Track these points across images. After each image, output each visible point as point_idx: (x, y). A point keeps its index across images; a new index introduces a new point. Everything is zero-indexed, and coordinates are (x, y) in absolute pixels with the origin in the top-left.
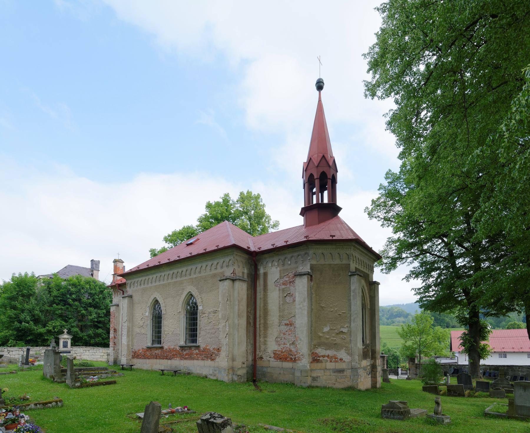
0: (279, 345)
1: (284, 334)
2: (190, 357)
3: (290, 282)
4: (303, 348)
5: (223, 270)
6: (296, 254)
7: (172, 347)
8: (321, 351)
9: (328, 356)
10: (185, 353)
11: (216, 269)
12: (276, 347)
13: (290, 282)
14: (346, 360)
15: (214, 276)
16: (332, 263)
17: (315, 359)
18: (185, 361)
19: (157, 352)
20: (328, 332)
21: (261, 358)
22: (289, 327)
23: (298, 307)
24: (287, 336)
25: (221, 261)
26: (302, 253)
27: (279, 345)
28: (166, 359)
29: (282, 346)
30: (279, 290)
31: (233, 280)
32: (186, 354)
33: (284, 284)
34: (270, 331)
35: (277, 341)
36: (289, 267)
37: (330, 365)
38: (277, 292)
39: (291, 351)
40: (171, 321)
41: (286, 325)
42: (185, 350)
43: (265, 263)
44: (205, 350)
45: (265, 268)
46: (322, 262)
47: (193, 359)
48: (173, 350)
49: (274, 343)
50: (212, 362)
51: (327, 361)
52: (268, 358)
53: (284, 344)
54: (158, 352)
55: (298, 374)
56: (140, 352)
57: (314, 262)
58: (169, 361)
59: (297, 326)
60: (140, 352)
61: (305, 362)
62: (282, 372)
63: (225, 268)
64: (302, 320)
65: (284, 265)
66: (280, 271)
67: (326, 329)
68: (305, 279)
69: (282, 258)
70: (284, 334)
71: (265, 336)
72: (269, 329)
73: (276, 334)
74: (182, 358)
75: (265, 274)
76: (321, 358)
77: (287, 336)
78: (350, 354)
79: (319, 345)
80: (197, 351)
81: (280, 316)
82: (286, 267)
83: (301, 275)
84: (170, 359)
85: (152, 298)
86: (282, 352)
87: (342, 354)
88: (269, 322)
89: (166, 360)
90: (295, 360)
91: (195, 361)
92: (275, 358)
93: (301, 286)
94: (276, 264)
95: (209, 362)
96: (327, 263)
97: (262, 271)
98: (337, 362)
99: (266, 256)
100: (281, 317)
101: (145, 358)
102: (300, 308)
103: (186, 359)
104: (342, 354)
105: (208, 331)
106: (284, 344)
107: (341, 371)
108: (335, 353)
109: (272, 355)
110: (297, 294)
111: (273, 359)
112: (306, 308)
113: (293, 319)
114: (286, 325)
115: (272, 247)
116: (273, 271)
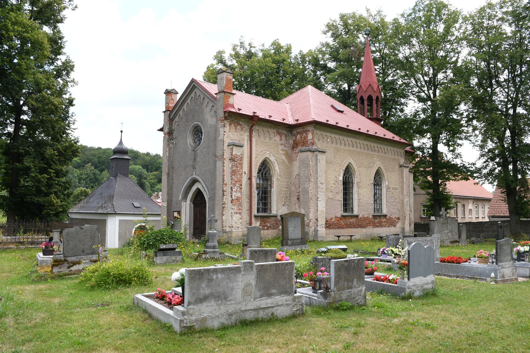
2: (381, 225)
7: (366, 216)
10: (376, 221)
19: (351, 220)
28: (361, 227)
32: (378, 222)
40: (365, 190)
47: (381, 226)
48: (367, 218)
54: (353, 220)
56: (333, 220)
58: (364, 230)
60: (333, 220)
74: (375, 226)
84: (364, 227)
89: (361, 229)
91: (384, 228)
101: (339, 228)
103: (377, 227)
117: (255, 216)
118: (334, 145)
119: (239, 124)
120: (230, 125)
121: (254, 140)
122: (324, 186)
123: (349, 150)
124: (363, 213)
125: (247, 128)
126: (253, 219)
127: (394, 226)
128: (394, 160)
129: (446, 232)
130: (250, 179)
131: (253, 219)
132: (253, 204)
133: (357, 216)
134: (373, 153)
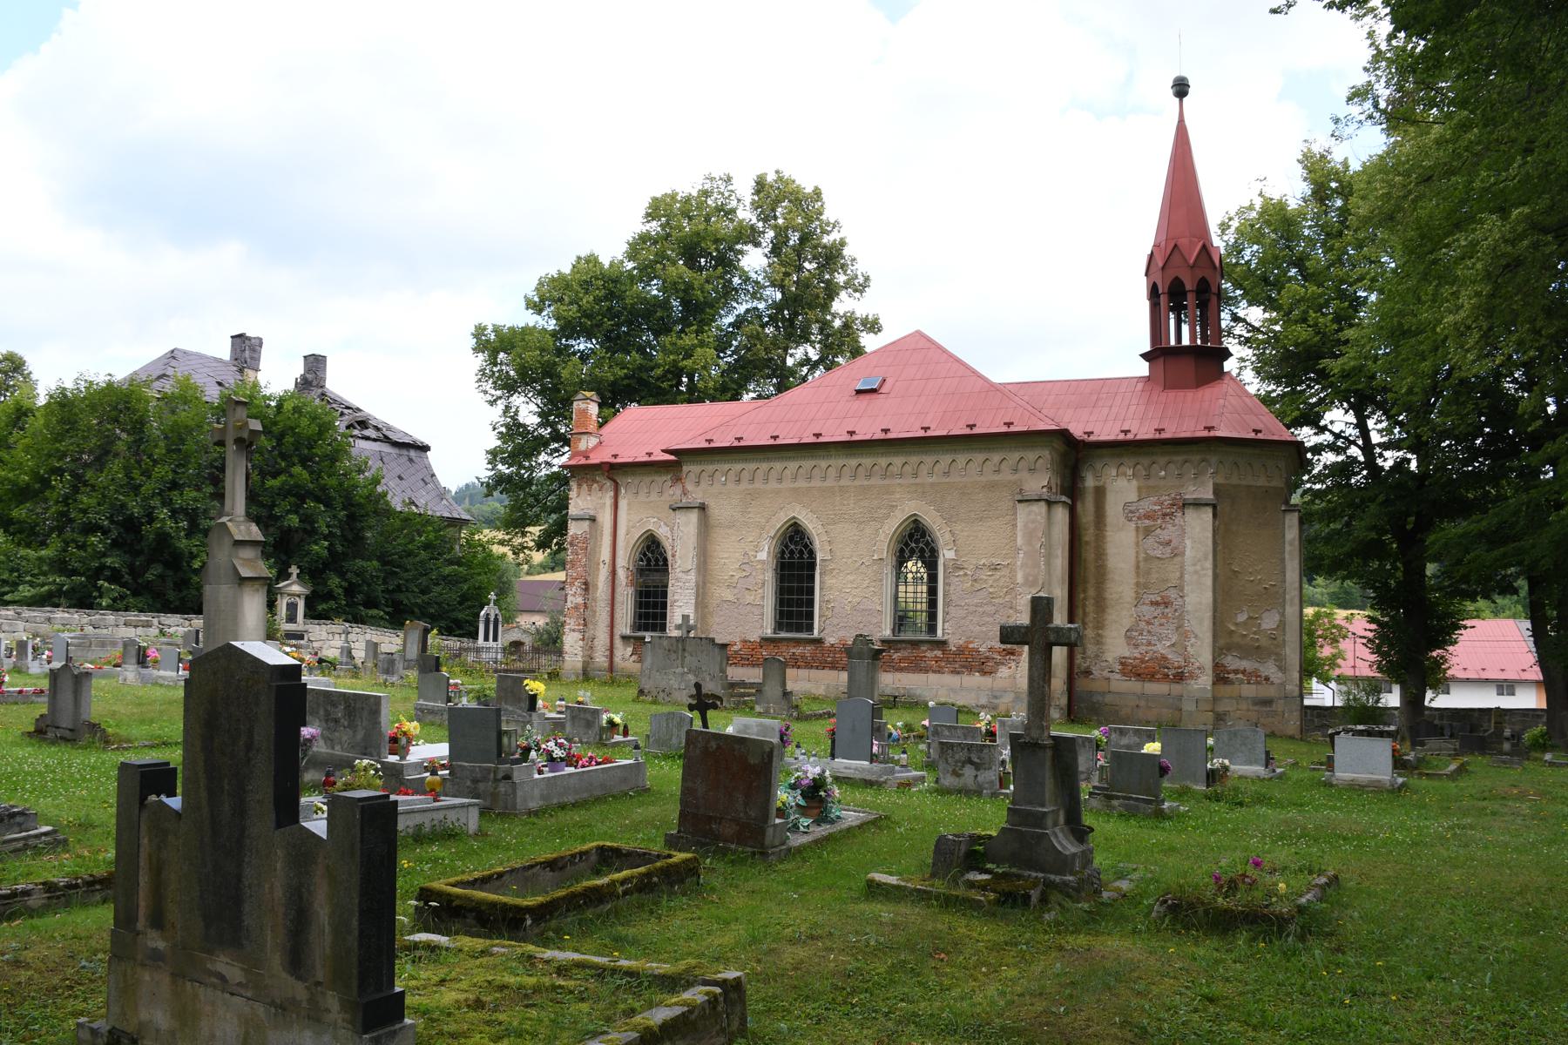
0: (1136, 646)
1: (1148, 623)
2: (917, 666)
3: (1165, 515)
4: (1202, 653)
5: (1016, 477)
6: (1180, 458)
8: (1231, 662)
9: (1244, 672)
11: (998, 471)
12: (1126, 651)
13: (1165, 515)
14: (1277, 681)
15: (992, 486)
16: (1252, 483)
17: (1221, 676)
18: (899, 675)
19: (798, 651)
20: (1245, 623)
21: (1088, 673)
22: (1160, 610)
23: (1189, 568)
24: (1155, 628)
25: (1016, 455)
26: (1197, 458)
27: (1136, 646)
28: (832, 668)
29: (1143, 649)
30: (1137, 528)
31: (1049, 503)
33: (1147, 517)
34: (1111, 615)
35: (1128, 638)
36: (1162, 483)
37: (1249, 690)
38: (1133, 534)
39: (1164, 658)
40: (850, 578)
41: (1157, 604)
42: (897, 650)
43: (1098, 465)
44: (961, 651)
45: (1097, 477)
46: (1235, 481)
49: (1122, 640)
50: (986, 681)
51: (1241, 682)
52: (1105, 673)
53: (1149, 644)
54: (808, 650)
55: (1188, 706)
57: (1220, 480)
59: (1189, 608)
61: (1204, 681)
62: (1142, 703)
63: (1024, 475)
64: (1198, 597)
65: (1148, 477)
66: (1139, 488)
67: (1242, 618)
68: (1207, 514)
69: (1146, 461)
70: (1148, 623)
71: (1100, 625)
72: (1109, 611)
73: (1127, 623)
75: (1100, 492)
76: (1231, 676)
77: (1155, 628)
78: (1282, 669)
79: (1229, 648)
80: (939, 653)
81: (1137, 584)
82: (1151, 482)
83: (1198, 504)
85: (779, 521)
86: (1143, 661)
87: (1270, 669)
88: (1107, 595)
90: (1180, 677)
91: (932, 677)
92: (1124, 674)
93: (1198, 529)
94: (1130, 472)
95: (976, 679)
96: (1244, 483)
97: (1090, 482)
98: (1258, 683)
99: (1104, 451)
100: (1141, 587)
102: (1196, 572)
103: (901, 670)
104: (1270, 669)
105: (972, 609)
106: (1149, 644)
107: (1267, 702)
108: (1257, 665)
109: (1118, 667)
110: (1188, 542)
111: (1118, 676)
112: (1210, 573)
113: (1173, 594)
114: (1157, 604)
115: (1121, 437)
116: (1121, 489)
117: (624, 638)
118: (744, 485)
119: (594, 481)
120: (579, 486)
121: (623, 504)
122: (692, 577)
123: (795, 490)
124: (842, 633)
125: (609, 483)
126: (618, 642)
127: (984, 673)
128: (992, 486)
129: (679, 670)
130: (614, 572)
131: (618, 642)
132: (618, 616)
133: (819, 641)
134: (886, 482)
